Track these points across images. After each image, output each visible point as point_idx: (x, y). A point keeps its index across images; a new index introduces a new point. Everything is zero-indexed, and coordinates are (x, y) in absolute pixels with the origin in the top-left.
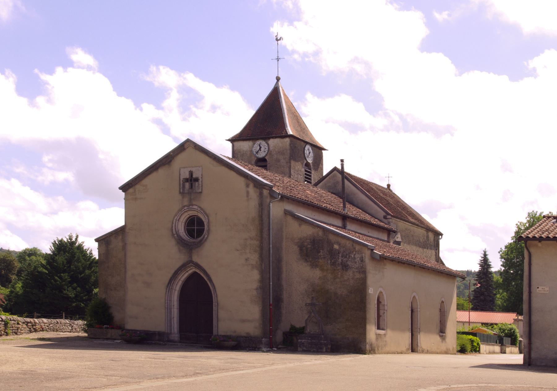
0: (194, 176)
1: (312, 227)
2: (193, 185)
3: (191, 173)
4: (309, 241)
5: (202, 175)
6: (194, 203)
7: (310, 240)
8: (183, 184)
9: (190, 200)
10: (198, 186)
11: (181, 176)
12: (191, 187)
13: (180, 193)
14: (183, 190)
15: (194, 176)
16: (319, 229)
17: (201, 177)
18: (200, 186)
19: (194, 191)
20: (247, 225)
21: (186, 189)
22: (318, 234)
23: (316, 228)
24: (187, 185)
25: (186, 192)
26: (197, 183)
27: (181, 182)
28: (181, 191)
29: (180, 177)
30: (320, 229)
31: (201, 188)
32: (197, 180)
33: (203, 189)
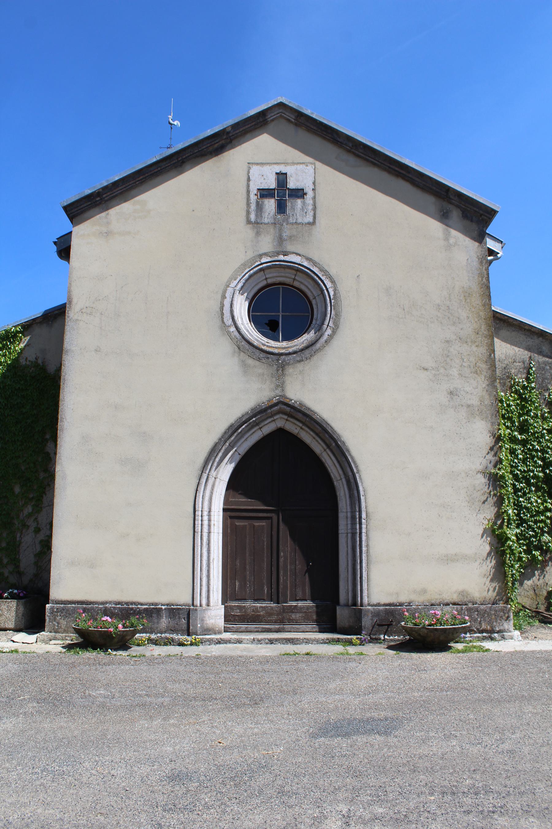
0: (292, 184)
1: (525, 335)
2: (289, 204)
3: (282, 178)
4: (520, 364)
5: (314, 183)
6: (290, 248)
7: (524, 363)
8: (257, 203)
9: (280, 240)
10: (302, 209)
11: (251, 183)
12: (281, 208)
13: (249, 222)
14: (257, 216)
15: (292, 184)
16: (541, 339)
17: (312, 187)
18: (310, 207)
19: (291, 220)
20: (448, 307)
21: (265, 215)
22: (540, 350)
23: (535, 337)
24: (270, 205)
25: (266, 221)
26: (299, 201)
27: (253, 198)
28: (253, 217)
29: (248, 186)
30: (544, 340)
31: (312, 213)
32: (299, 193)
33: (317, 215)
